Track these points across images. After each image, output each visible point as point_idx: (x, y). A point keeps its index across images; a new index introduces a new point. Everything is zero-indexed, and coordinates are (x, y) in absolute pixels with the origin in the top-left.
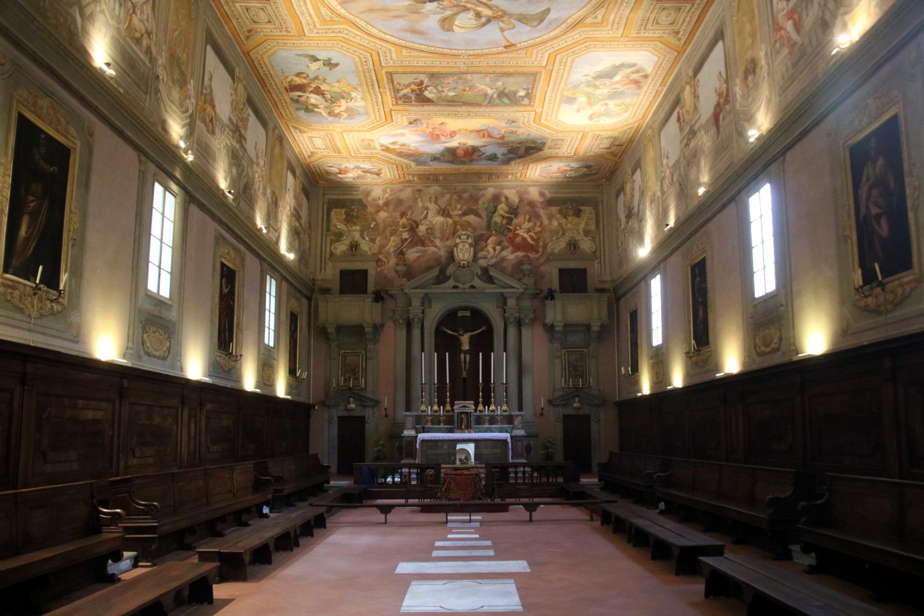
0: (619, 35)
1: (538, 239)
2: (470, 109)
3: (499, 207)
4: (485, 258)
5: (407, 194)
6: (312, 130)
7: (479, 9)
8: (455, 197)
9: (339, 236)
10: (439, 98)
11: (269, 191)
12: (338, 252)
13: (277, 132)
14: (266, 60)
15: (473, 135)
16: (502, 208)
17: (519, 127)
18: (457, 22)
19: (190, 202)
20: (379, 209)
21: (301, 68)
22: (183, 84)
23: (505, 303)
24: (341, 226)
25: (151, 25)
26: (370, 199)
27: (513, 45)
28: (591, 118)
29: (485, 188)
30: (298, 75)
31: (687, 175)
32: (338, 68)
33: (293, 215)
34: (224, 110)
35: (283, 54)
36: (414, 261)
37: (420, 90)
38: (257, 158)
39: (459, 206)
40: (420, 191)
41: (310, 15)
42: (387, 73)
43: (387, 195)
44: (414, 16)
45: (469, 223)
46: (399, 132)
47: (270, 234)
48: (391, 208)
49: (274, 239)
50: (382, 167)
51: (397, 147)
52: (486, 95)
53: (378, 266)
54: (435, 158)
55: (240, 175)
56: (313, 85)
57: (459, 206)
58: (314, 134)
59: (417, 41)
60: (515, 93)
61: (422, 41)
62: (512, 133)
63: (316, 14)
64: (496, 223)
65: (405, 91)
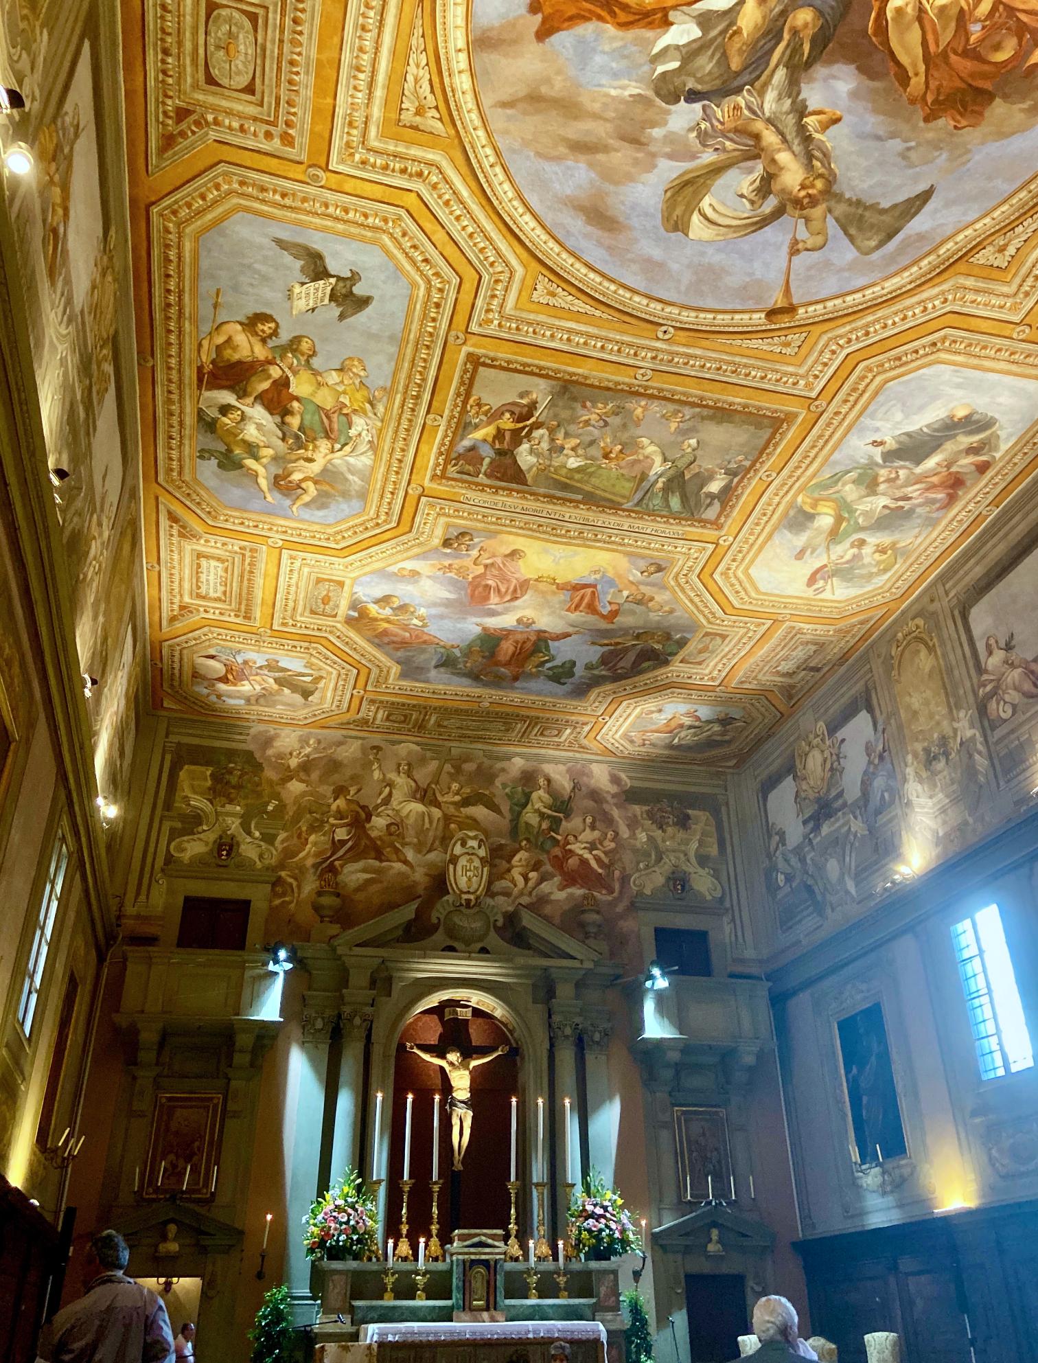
1: (612, 863)
3: (535, 796)
4: (507, 894)
5: (350, 752)
6: (214, 530)
7: (784, 157)
8: (448, 767)
10: (542, 471)
15: (563, 596)
16: (540, 798)
20: (288, 775)
21: (265, 298)
23: (551, 993)
26: (270, 752)
29: (508, 758)
30: (253, 322)
32: (369, 310)
36: (359, 889)
37: (516, 433)
39: (455, 786)
40: (377, 748)
41: (371, 85)
43: (308, 750)
44: (621, 156)
45: (475, 820)
46: (409, 565)
48: (315, 775)
53: (275, 894)
57: (455, 786)
58: (212, 545)
61: (595, 255)
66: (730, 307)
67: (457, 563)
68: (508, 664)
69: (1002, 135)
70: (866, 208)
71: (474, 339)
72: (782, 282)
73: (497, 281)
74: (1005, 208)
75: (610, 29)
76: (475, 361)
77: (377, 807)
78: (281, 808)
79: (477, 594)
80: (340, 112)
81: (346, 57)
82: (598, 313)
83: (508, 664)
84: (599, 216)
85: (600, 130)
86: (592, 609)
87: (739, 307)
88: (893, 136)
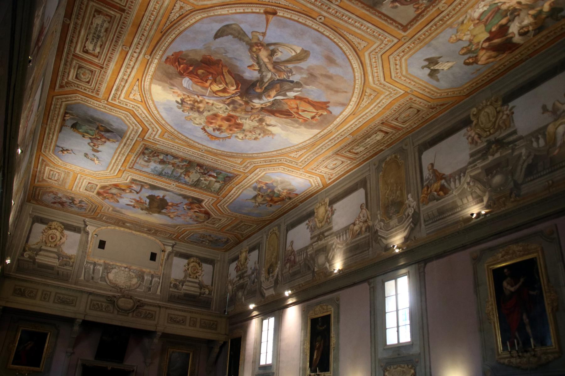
7: (266, 60)
18: (294, 54)
27: (266, 13)
41: (379, 103)
44: (317, 73)
61: (337, 51)
66: (291, 22)
69: (195, 51)
70: (237, 37)
71: (399, 37)
72: (269, 26)
73: (377, 53)
74: (186, 25)
75: (310, 99)
76: (405, 28)
80: (392, 99)
81: (381, 109)
82: (345, 33)
84: (330, 60)
87: (288, 20)
88: (231, 58)
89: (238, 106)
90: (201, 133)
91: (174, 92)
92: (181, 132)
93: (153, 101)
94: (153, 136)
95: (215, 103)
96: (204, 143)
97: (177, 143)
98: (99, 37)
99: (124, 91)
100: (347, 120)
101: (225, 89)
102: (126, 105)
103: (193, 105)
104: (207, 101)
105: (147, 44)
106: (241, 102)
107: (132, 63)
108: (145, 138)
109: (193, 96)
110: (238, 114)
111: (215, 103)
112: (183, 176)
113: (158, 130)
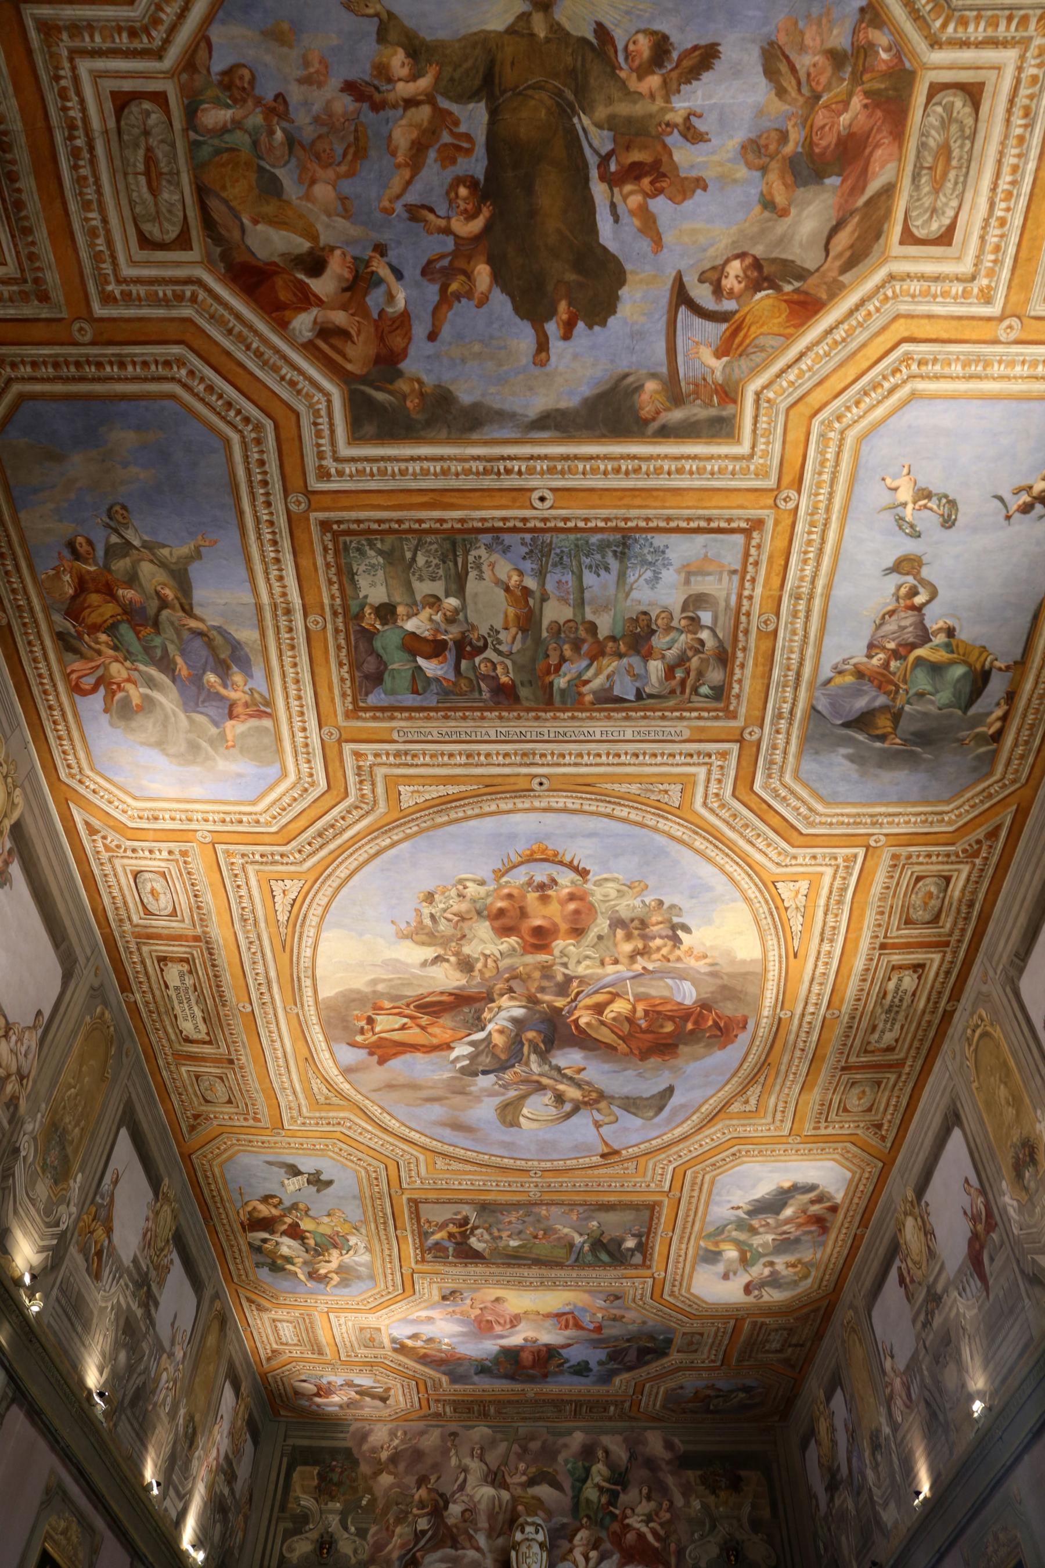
0: (786, 1132)
2: (544, 1271)
5: (431, 1440)
7: (561, 1087)
8: (516, 1448)
9: (302, 1520)
10: (494, 1250)
11: (182, 1412)
12: (294, 1557)
13: (218, 1305)
14: (216, 1170)
15: (549, 1322)
17: (628, 1309)
18: (525, 1111)
19: (13, 1401)
20: (380, 1468)
21: (270, 1187)
22: (61, 1175)
24: (307, 1502)
25: (30, 1065)
26: (365, 1447)
27: (616, 1152)
28: (747, 1289)
30: (266, 1199)
31: (938, 1383)
32: (331, 1190)
33: (220, 1469)
34: (127, 1239)
35: (244, 1159)
38: (173, 1344)
40: (454, 1434)
41: (294, 1092)
42: (409, 1200)
43: (396, 1442)
44: (458, 1099)
45: (539, 1499)
46: (424, 1314)
47: (167, 1503)
48: (402, 1467)
49: (174, 1515)
50: (391, 1383)
51: (419, 1343)
52: (571, 1245)
54: (483, 1369)
55: (130, 1368)
56: (288, 1220)
57: (522, 1466)
58: (280, 1314)
59: (461, 1144)
60: (619, 1242)
61: (468, 1144)
62: (615, 1319)
63: (304, 1090)
64: (588, 1501)
65: (437, 1236)
67: (458, 1309)
68: (533, 1367)
69: (696, 1058)
75: (419, 1055)
77: (454, 1493)
78: (373, 1501)
79: (483, 1327)
80: (283, 1105)
83: (533, 1367)
85: (440, 1093)
86: (578, 1326)
89: (545, 983)
90: (580, 851)
91: (705, 957)
92: (637, 830)
93: (747, 899)
94: (715, 776)
95: (600, 971)
96: (550, 818)
97: (630, 778)
98: (889, 1011)
99: (825, 892)
100: (301, 1043)
101: (600, 1013)
102: (814, 857)
103: (645, 937)
104: (619, 967)
105: (792, 1037)
106: (547, 998)
107: (816, 989)
108: (735, 747)
109: (657, 964)
110: (530, 959)
111: (600, 971)
112: (531, 583)
113: (705, 804)
